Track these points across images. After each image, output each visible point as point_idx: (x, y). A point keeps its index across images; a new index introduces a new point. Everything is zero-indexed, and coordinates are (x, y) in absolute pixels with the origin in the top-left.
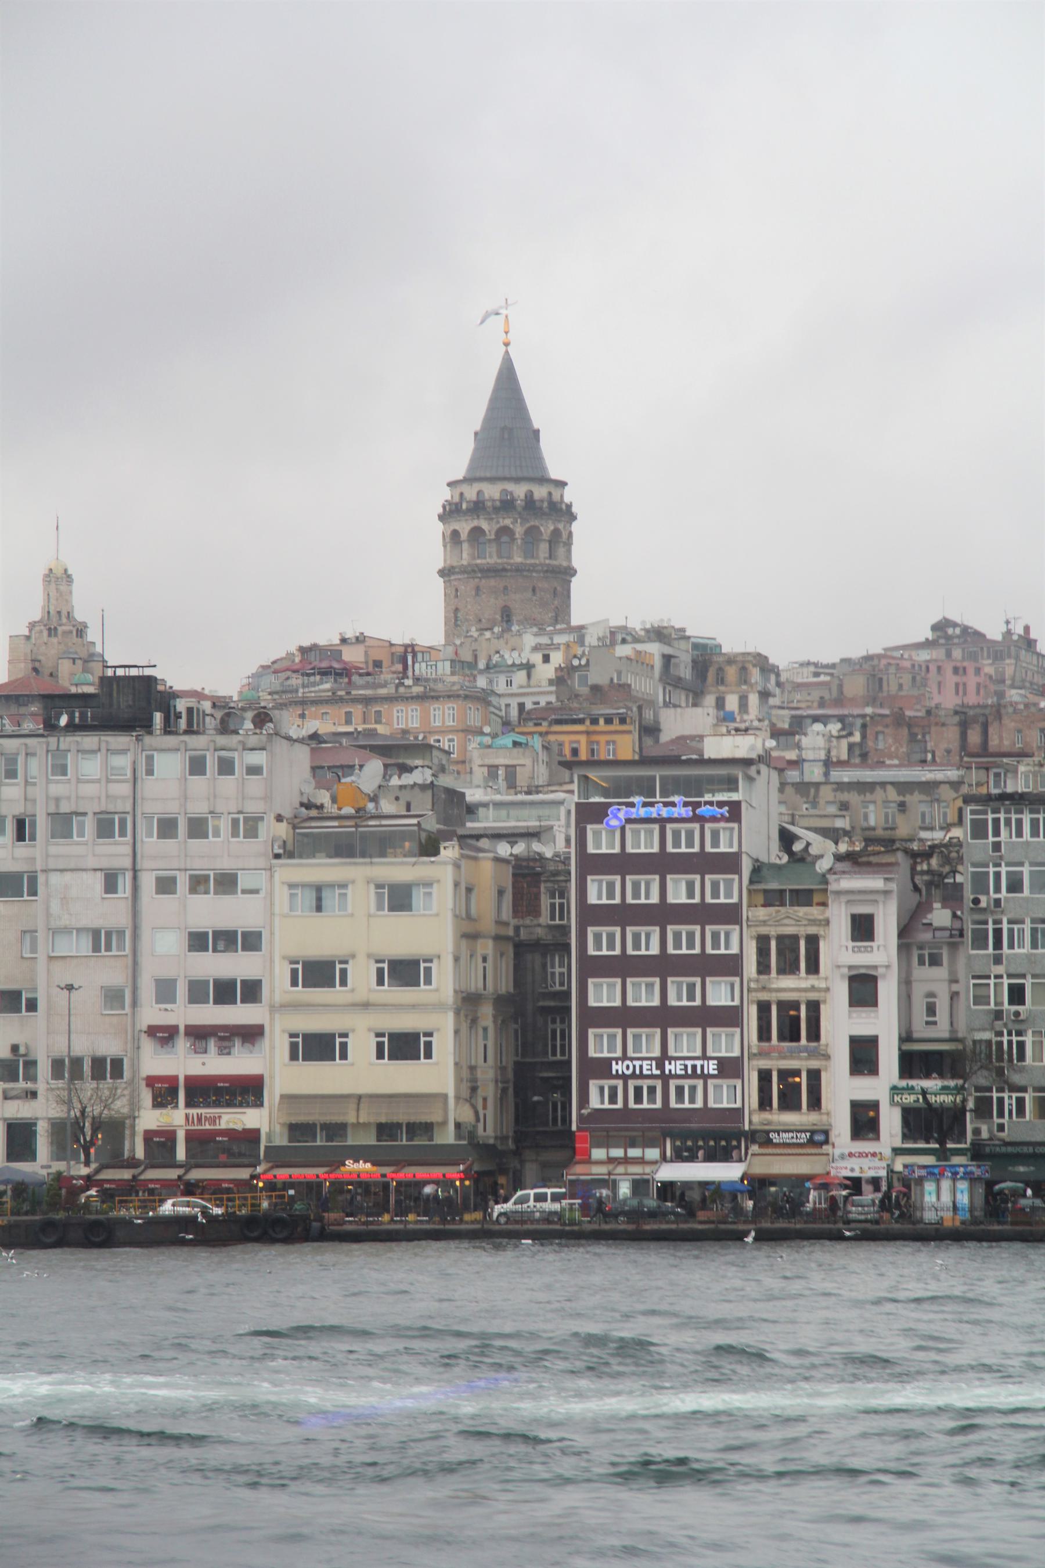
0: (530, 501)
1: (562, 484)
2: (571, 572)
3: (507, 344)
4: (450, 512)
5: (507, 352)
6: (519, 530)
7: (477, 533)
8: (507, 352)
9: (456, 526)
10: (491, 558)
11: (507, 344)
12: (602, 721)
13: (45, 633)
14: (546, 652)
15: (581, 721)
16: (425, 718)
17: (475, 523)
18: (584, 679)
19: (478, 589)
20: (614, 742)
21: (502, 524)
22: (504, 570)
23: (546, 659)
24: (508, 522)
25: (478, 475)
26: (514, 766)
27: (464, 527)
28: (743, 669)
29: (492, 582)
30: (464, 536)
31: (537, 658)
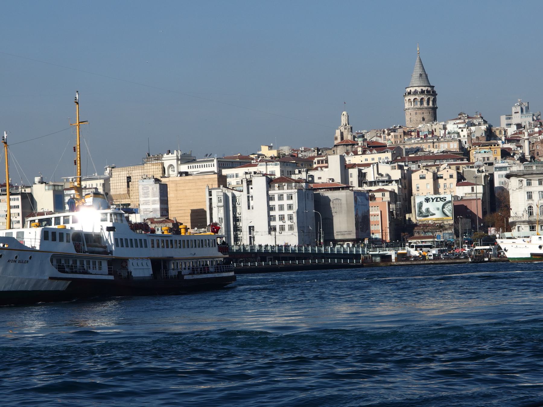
1: (433, 87)
2: (437, 108)
12: (493, 145)
13: (344, 129)
14: (462, 129)
15: (488, 146)
16: (449, 146)
18: (474, 136)
20: (496, 150)
21: (422, 97)
23: (462, 131)
24: (423, 97)
26: (489, 157)
28: (500, 131)
29: (420, 111)
30: (412, 100)
31: (460, 131)
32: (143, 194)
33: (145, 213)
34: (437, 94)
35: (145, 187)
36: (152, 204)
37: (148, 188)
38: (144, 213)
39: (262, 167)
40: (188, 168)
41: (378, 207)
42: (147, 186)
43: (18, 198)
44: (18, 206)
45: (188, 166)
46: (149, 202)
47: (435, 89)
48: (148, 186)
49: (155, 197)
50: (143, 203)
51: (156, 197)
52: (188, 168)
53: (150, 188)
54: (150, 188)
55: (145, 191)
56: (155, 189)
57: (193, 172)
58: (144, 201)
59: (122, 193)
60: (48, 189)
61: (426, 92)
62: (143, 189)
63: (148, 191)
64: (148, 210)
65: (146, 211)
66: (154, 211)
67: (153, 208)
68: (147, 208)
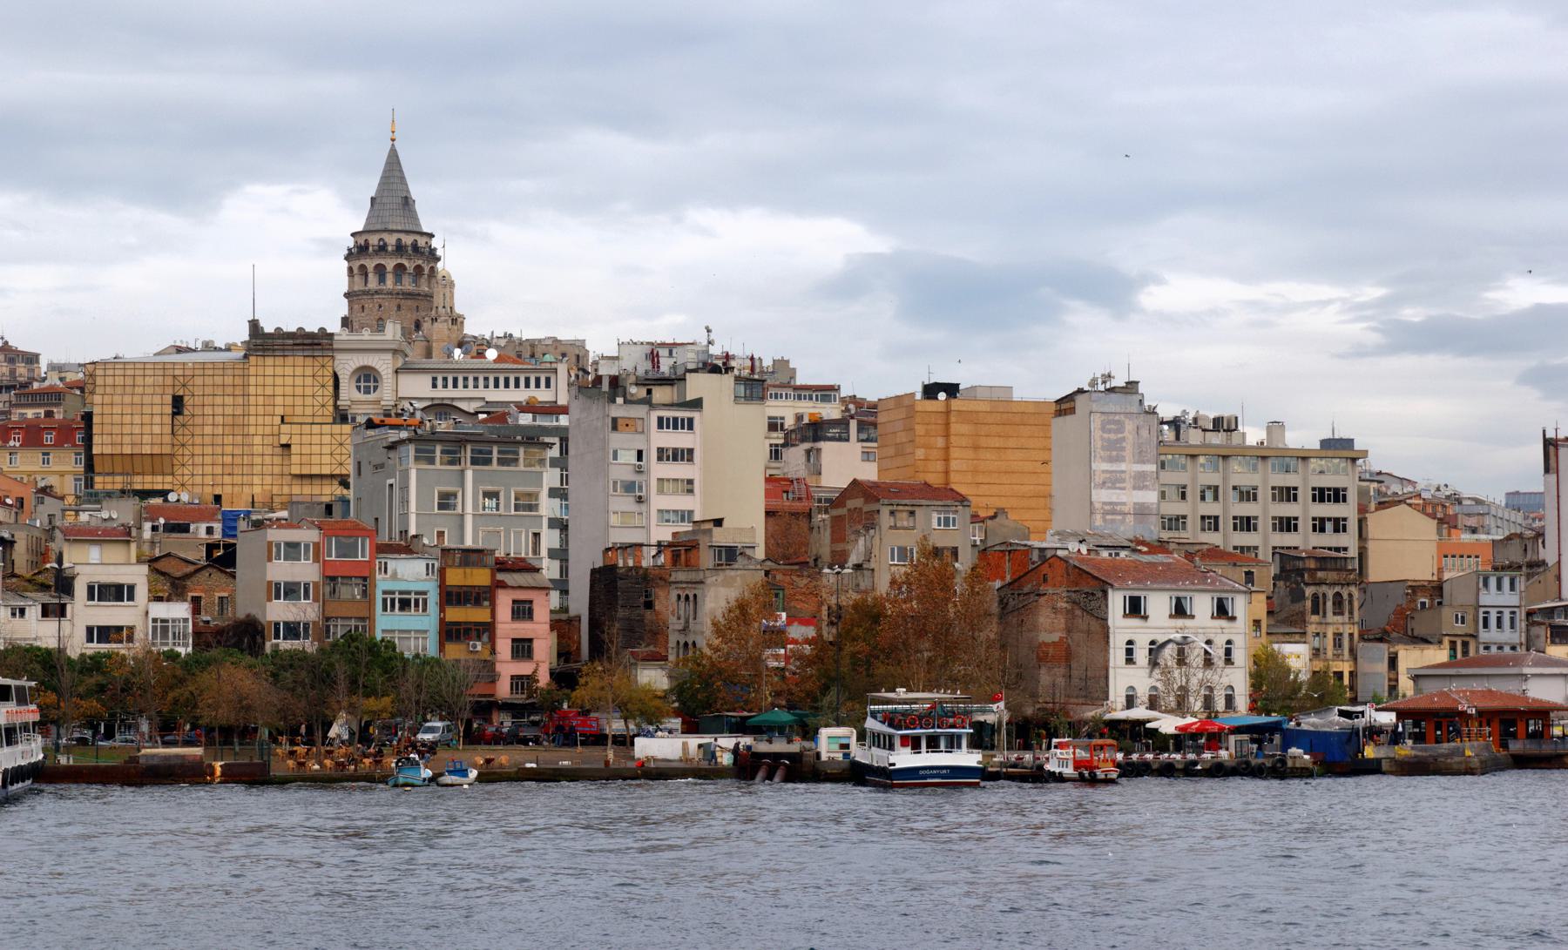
0: (415, 246)
3: (393, 140)
4: (359, 251)
5: (393, 145)
6: (426, 271)
7: (400, 269)
8: (393, 145)
9: (383, 262)
10: (407, 285)
11: (393, 140)
17: (399, 261)
19: (399, 307)
22: (419, 295)
24: (420, 262)
25: (371, 228)
27: (390, 264)
29: (409, 302)
32: (1103, 448)
33: (1109, 517)
34: (438, 259)
35: (1109, 422)
36: (1135, 488)
37: (1121, 430)
38: (1105, 520)
39: (779, 402)
40: (434, 386)
41: (1477, 557)
42: (1117, 418)
43: (691, 421)
44: (691, 451)
45: (435, 379)
46: (1123, 481)
47: (435, 243)
48: (1122, 417)
49: (1138, 463)
50: (1104, 483)
51: (1148, 462)
52: (434, 386)
53: (1129, 426)
54: (1129, 426)
55: (1113, 436)
56: (1144, 433)
57: (453, 399)
58: (1108, 476)
59: (147, 450)
60: (745, 397)
61: (409, 248)
62: (1103, 429)
63: (1120, 436)
64: (1118, 508)
65: (1114, 512)
66: (1141, 512)
67: (1135, 504)
68: (1114, 499)
